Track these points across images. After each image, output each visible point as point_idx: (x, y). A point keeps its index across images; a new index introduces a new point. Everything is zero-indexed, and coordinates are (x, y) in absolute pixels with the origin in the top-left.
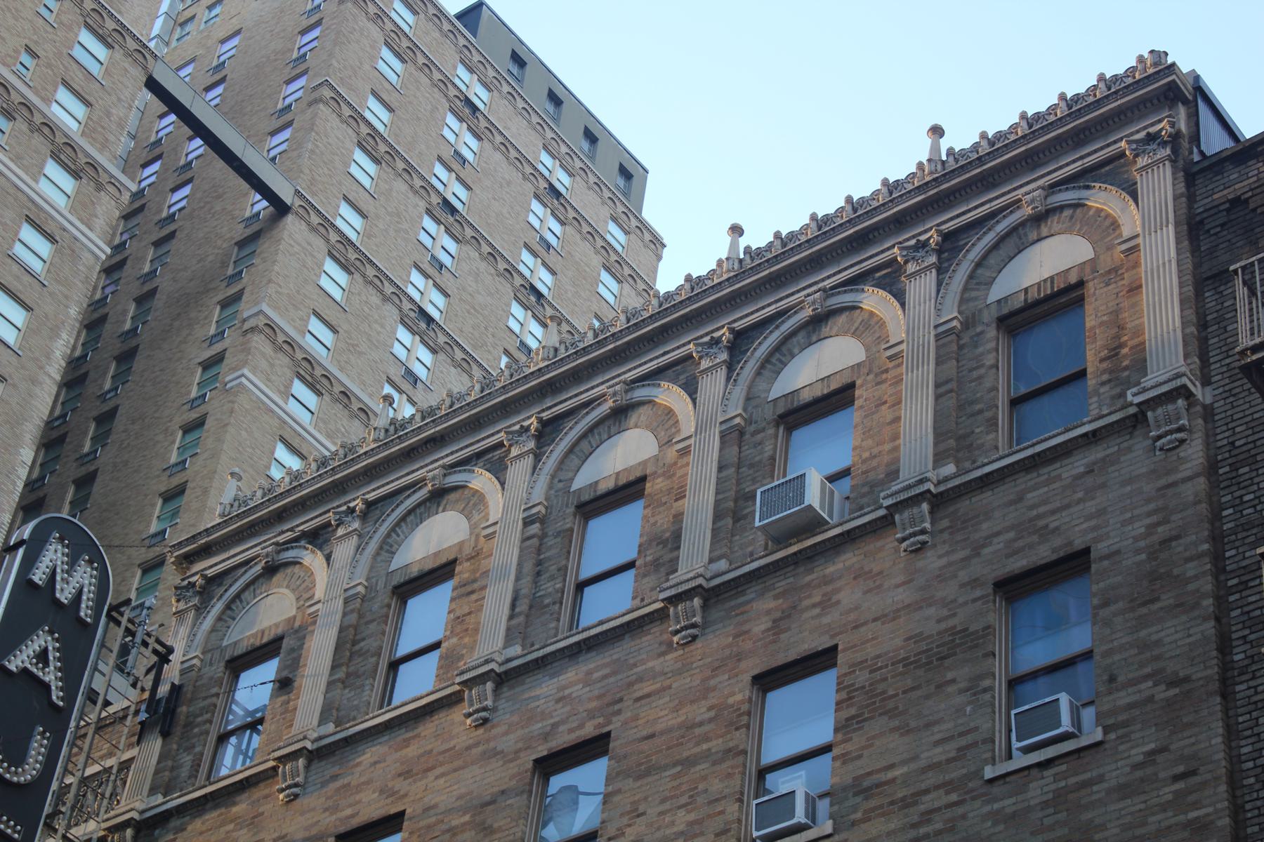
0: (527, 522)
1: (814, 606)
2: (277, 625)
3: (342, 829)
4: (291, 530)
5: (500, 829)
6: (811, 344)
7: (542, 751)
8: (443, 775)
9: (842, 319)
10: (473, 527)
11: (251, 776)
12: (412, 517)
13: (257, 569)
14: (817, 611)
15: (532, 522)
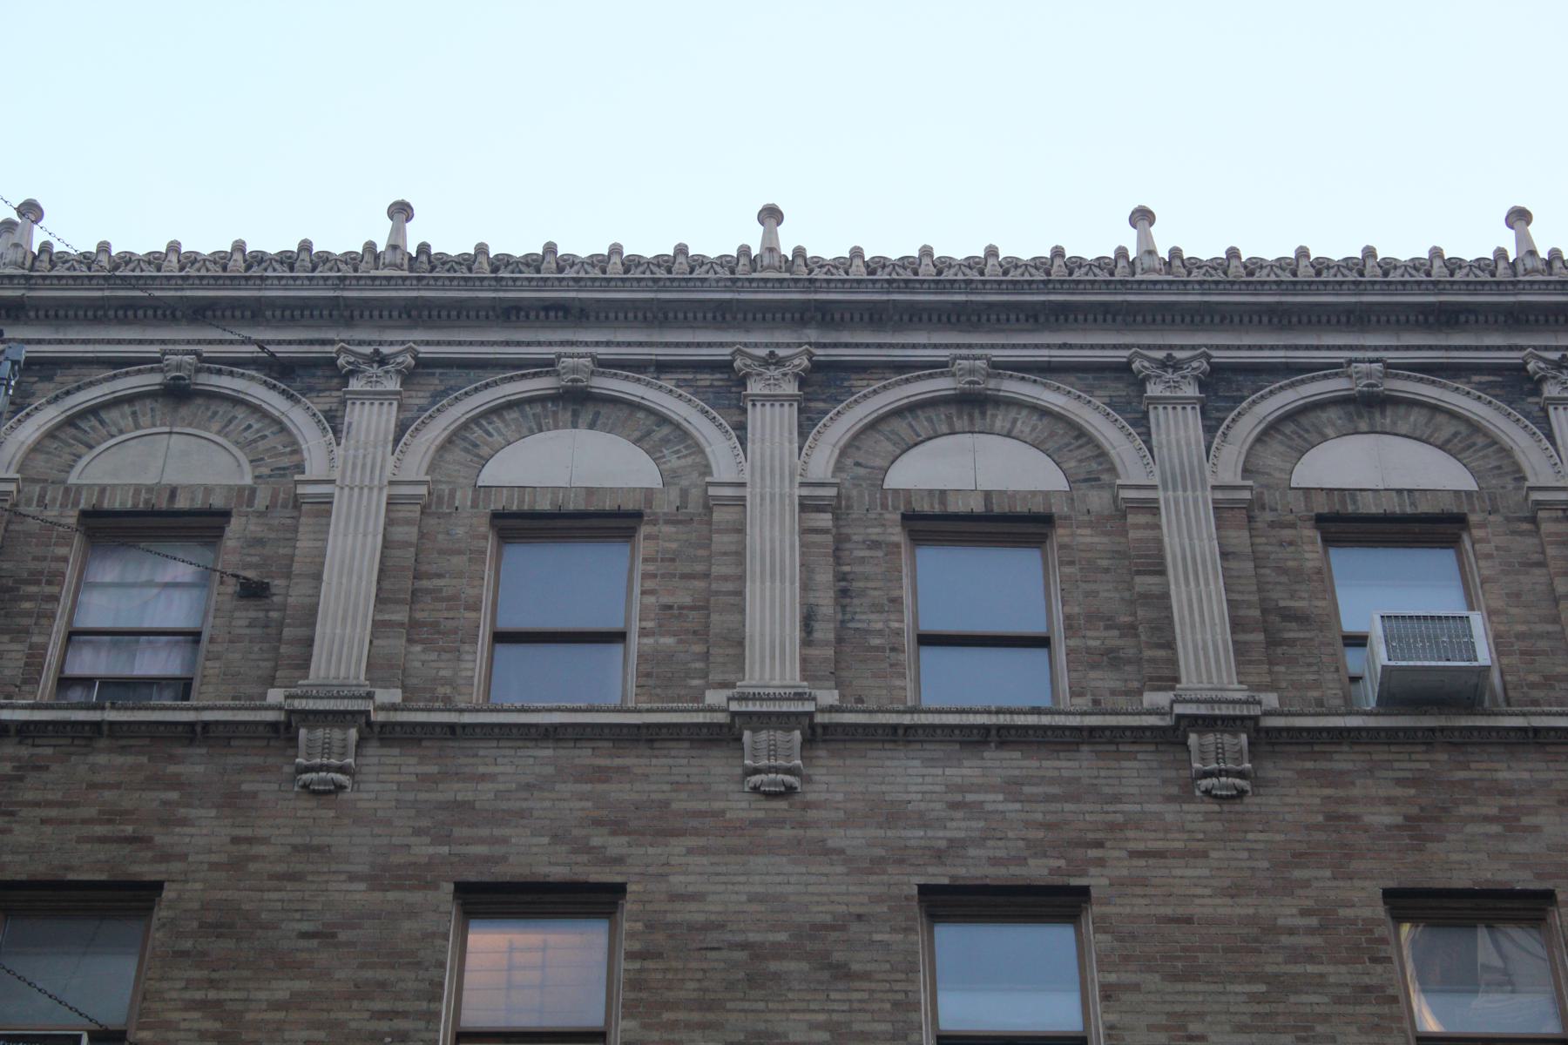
0: (806, 506)
1: (1487, 819)
2: (208, 490)
3: (471, 876)
4: (261, 344)
5: (866, 976)
6: (1357, 433)
7: (939, 875)
8: (704, 851)
9: (1417, 417)
10: (669, 478)
11: (217, 723)
12: (512, 415)
13: (153, 380)
14: (1495, 828)
15: (819, 509)
